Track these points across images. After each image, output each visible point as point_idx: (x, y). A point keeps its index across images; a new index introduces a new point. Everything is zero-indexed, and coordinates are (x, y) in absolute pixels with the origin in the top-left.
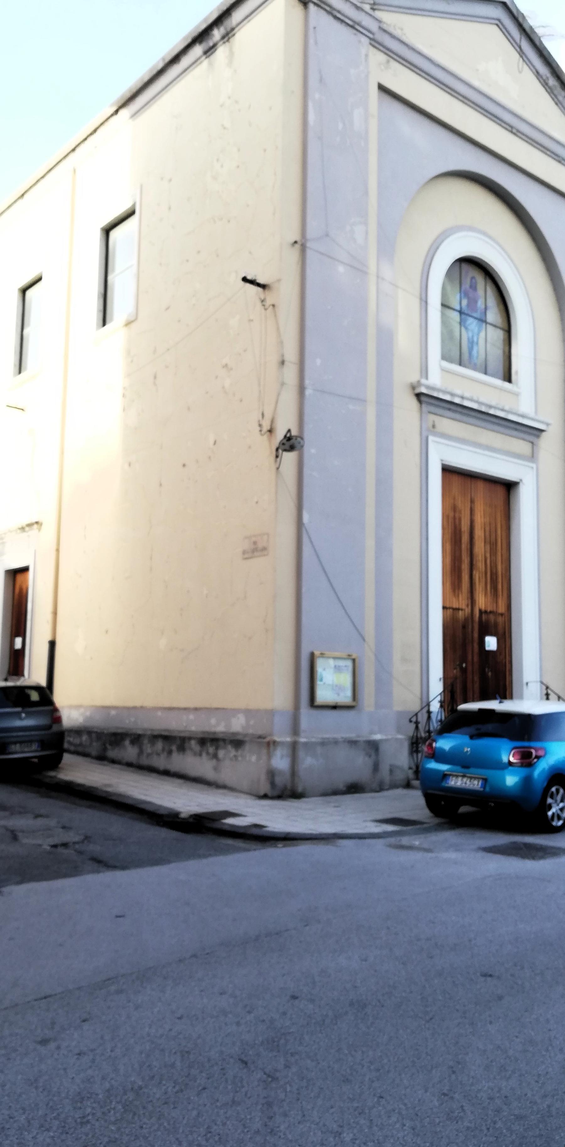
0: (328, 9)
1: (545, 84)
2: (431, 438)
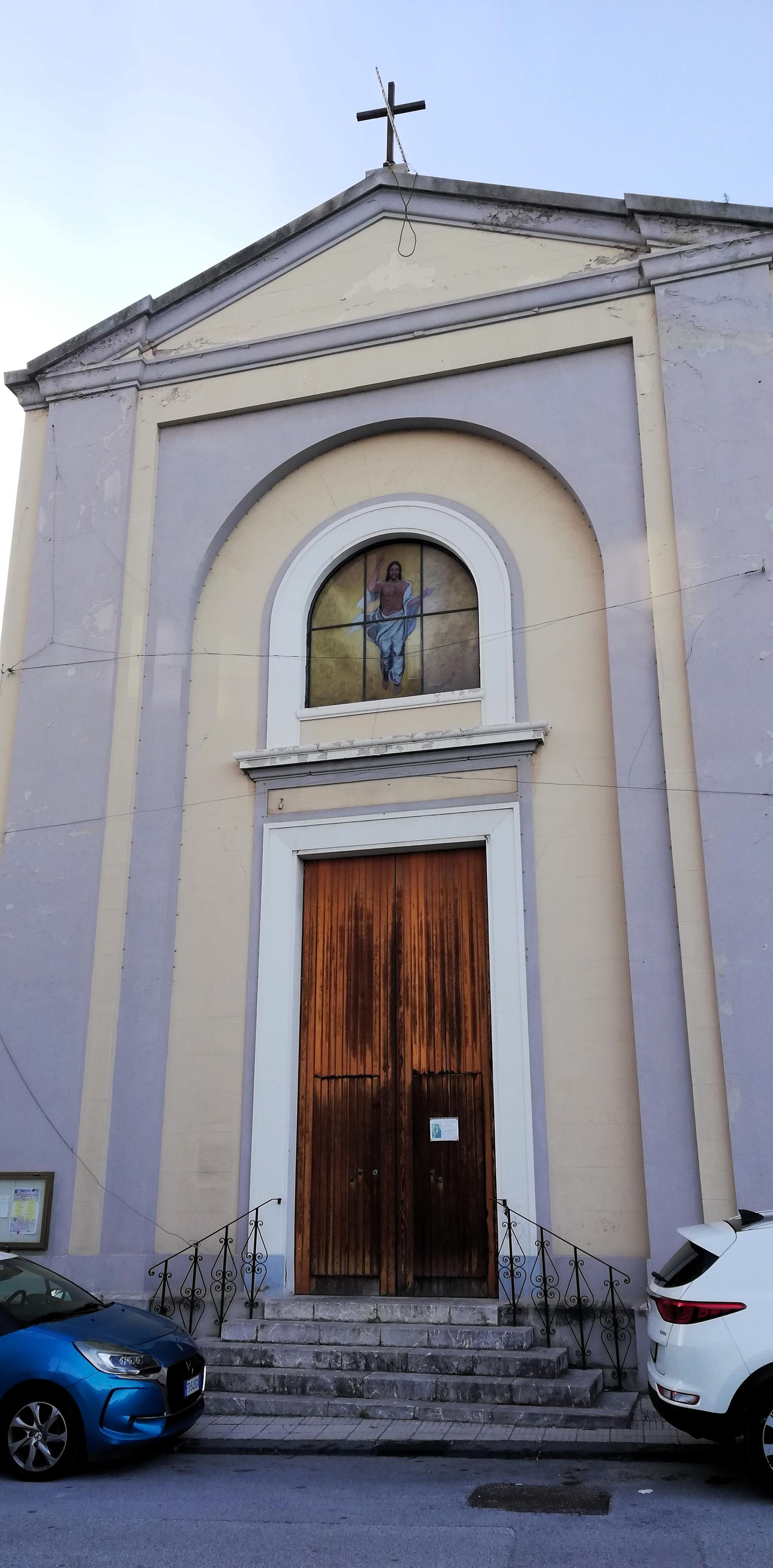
0: (71, 395)
1: (494, 227)
2: (267, 826)
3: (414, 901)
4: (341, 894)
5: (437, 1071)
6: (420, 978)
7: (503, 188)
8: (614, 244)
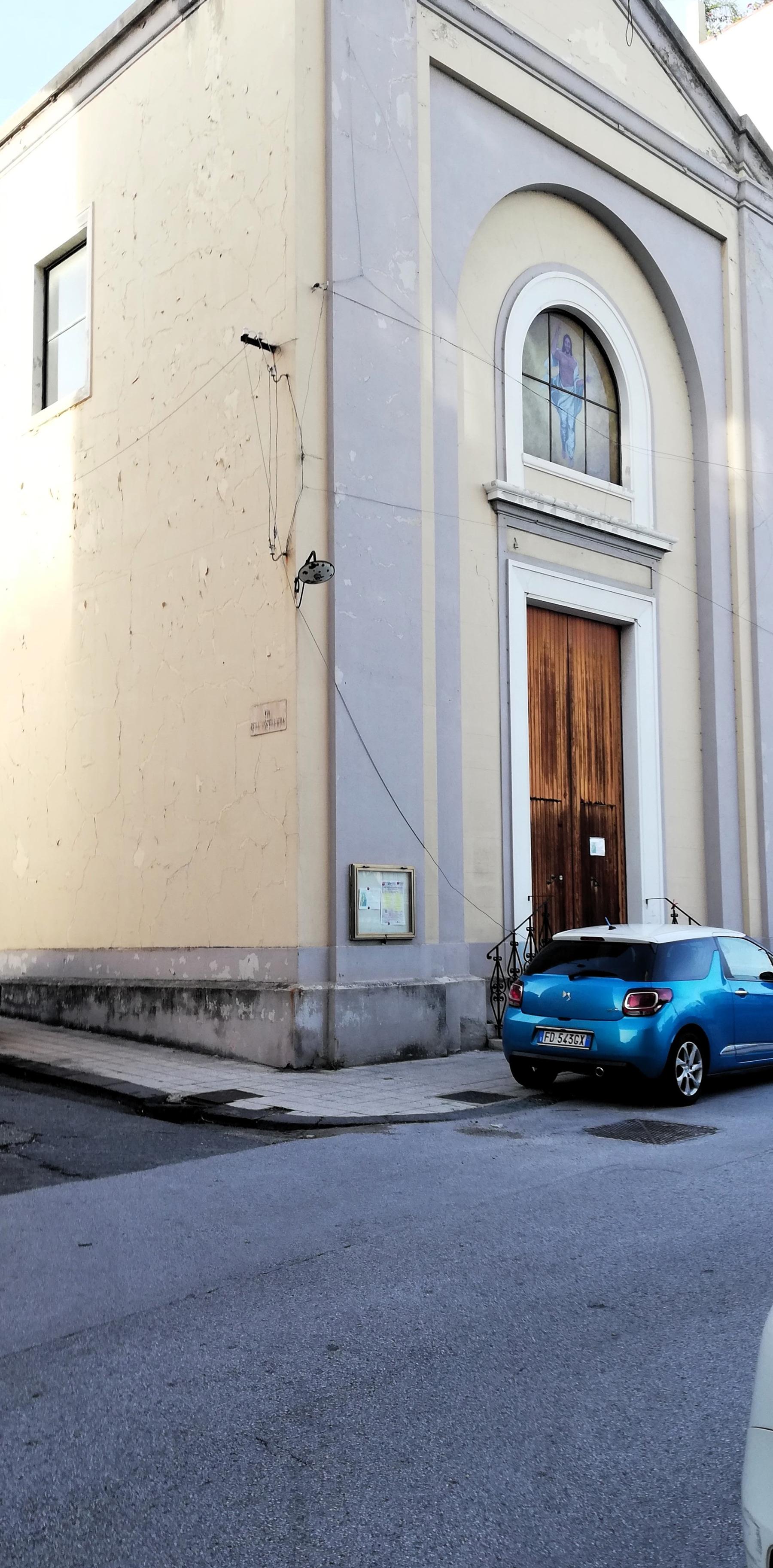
1: (663, 63)
2: (511, 563)
3: (579, 660)
4: (536, 641)
5: (594, 802)
6: (583, 726)
7: (681, 34)
8: (723, 147)
